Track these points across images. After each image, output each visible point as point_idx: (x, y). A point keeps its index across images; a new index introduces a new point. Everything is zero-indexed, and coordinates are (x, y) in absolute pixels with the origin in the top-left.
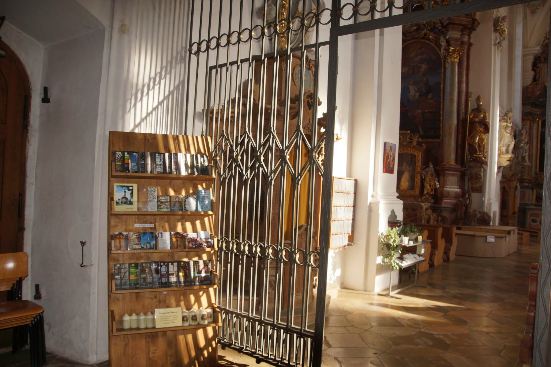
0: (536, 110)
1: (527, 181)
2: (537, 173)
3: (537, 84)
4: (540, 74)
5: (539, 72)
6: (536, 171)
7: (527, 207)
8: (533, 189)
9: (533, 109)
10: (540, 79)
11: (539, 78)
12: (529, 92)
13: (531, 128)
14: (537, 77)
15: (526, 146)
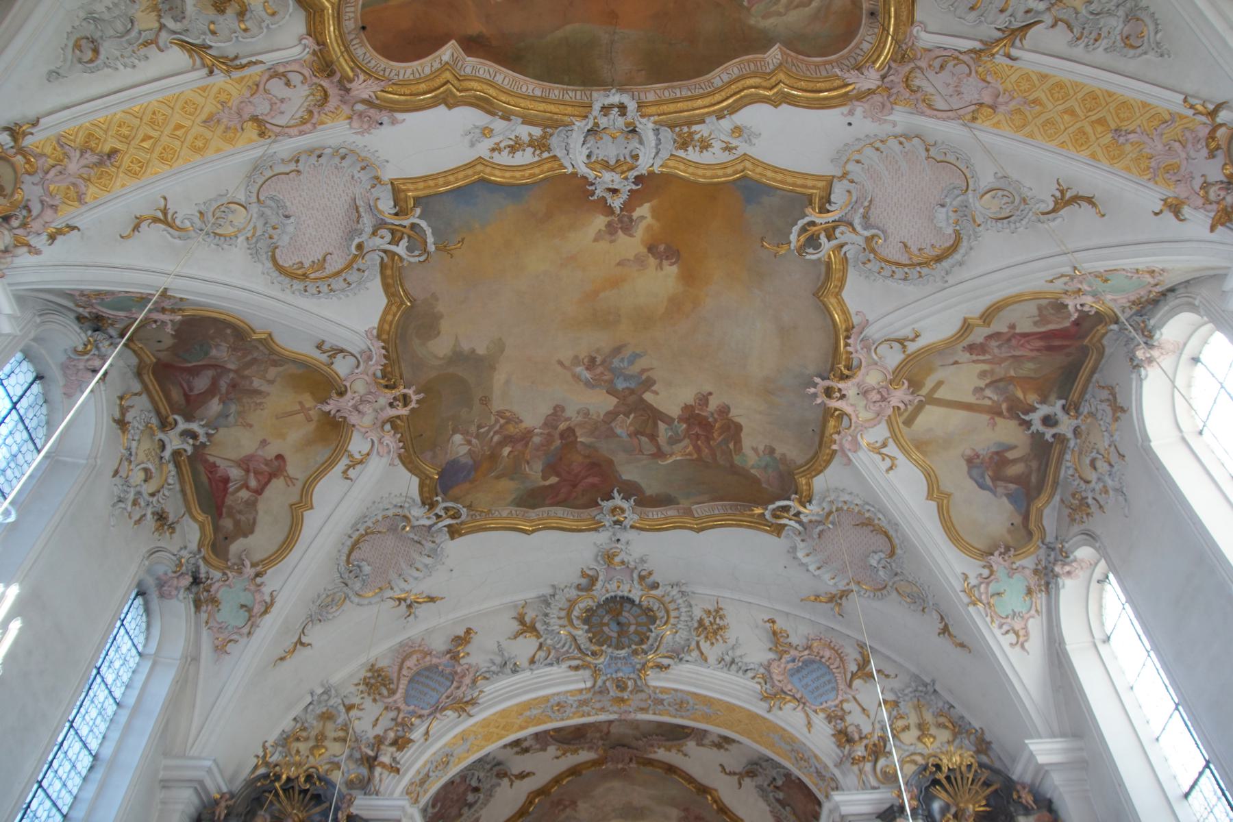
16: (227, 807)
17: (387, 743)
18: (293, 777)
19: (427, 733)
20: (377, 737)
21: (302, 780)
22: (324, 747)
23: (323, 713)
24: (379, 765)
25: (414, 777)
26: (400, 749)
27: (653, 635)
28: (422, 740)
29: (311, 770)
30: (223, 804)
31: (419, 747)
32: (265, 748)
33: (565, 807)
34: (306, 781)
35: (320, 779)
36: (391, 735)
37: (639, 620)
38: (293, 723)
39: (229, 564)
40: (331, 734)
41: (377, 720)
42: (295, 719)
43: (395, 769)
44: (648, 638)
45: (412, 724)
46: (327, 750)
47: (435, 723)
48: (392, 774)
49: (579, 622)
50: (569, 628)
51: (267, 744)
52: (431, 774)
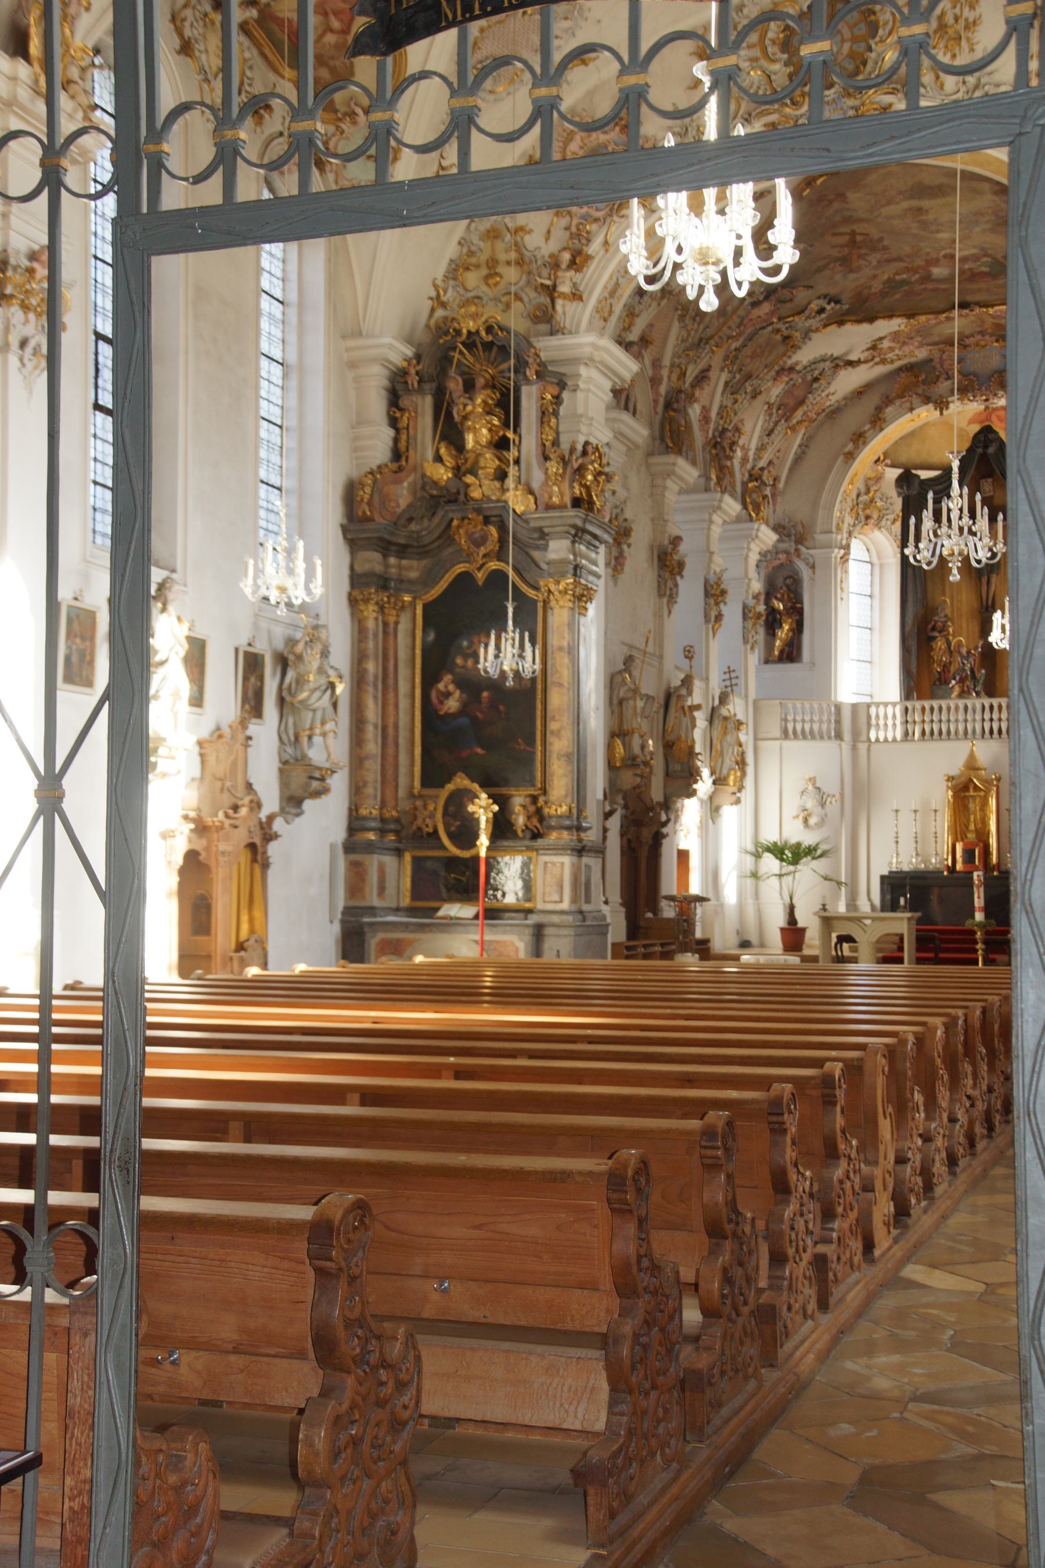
0: (404, 562)
1: (373, 824)
2: (416, 791)
3: (400, 469)
4: (411, 432)
5: (408, 429)
6: (412, 786)
7: (366, 920)
8: (399, 852)
9: (392, 560)
10: (411, 452)
11: (407, 450)
12: (362, 500)
13: (388, 630)
14: (402, 445)
15: (320, 698)
16: (417, 373)
17: (564, 266)
18: (473, 330)
19: (606, 243)
20: (552, 256)
21: (483, 333)
22: (497, 274)
23: (488, 231)
24: (559, 297)
25: (601, 294)
26: (579, 270)
27: (873, 55)
28: (603, 251)
29: (491, 320)
30: (413, 371)
31: (600, 261)
32: (435, 286)
33: (831, 202)
34: (487, 333)
35: (501, 328)
36: (566, 256)
37: (856, 31)
38: (459, 247)
39: (339, 115)
40: (502, 257)
41: (549, 232)
42: (460, 243)
43: (576, 296)
44: (865, 63)
45: (588, 232)
46: (501, 277)
47: (613, 228)
48: (575, 303)
49: (776, 49)
50: (763, 63)
51: (439, 282)
52: (621, 280)
